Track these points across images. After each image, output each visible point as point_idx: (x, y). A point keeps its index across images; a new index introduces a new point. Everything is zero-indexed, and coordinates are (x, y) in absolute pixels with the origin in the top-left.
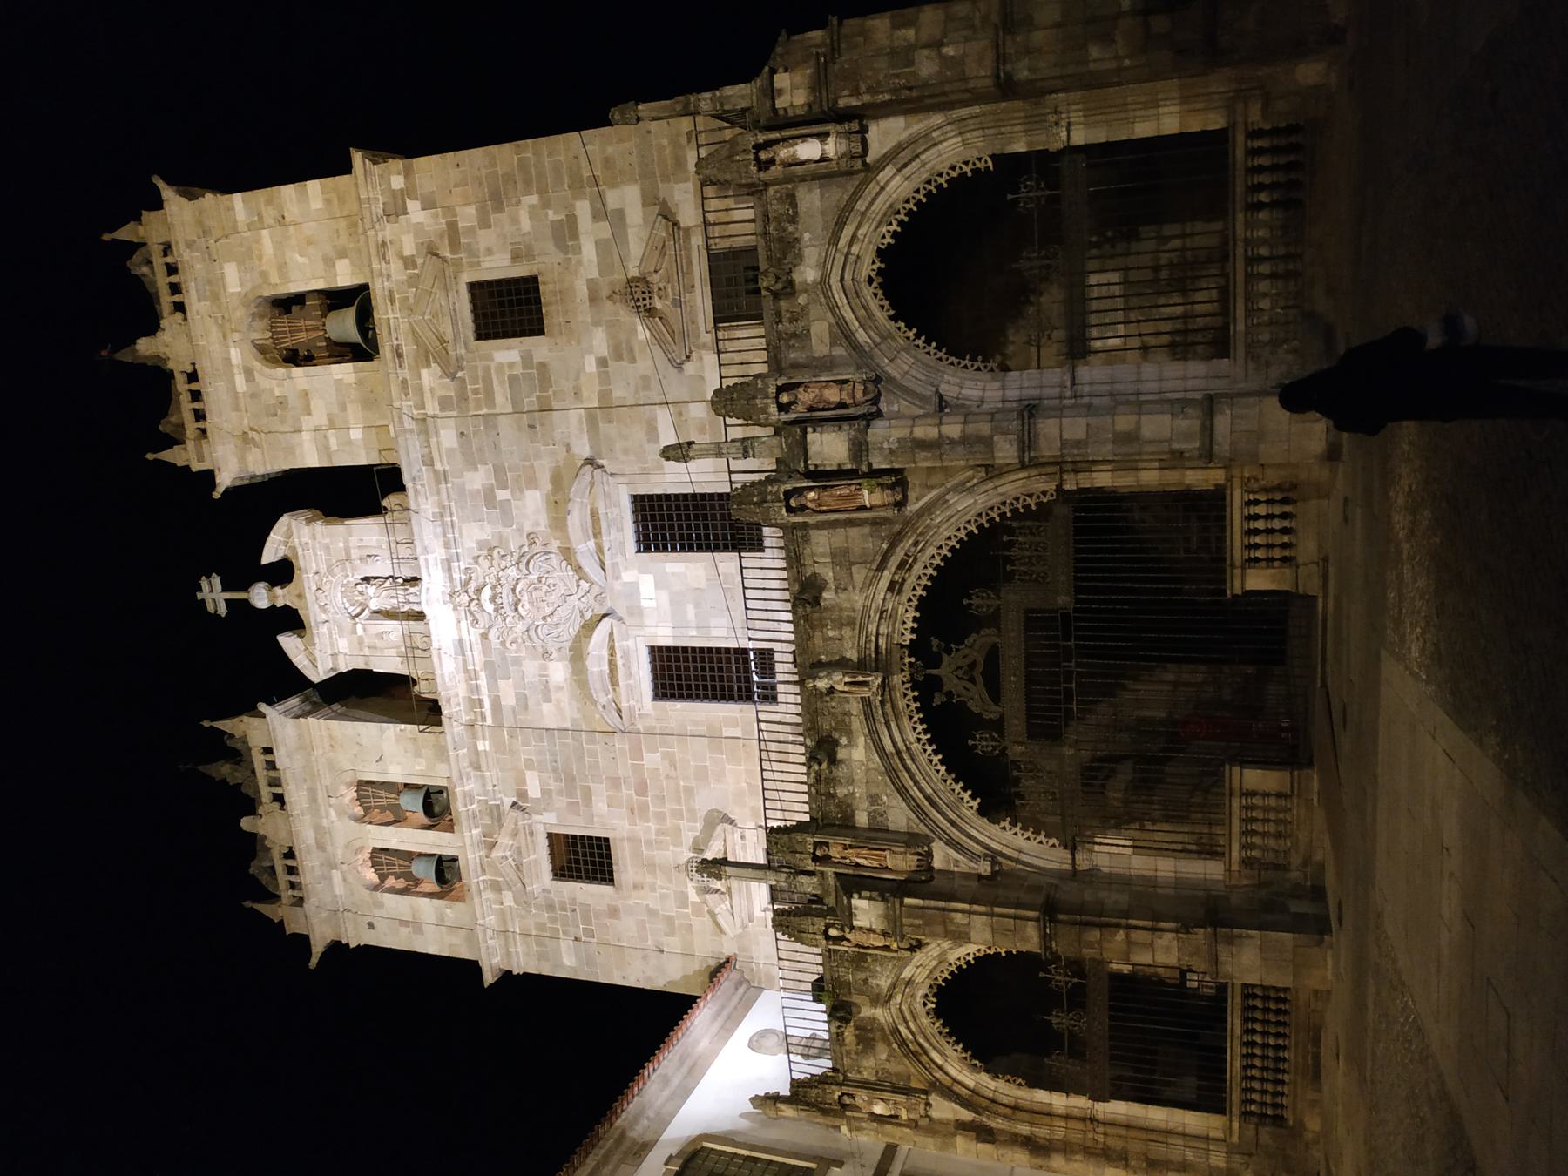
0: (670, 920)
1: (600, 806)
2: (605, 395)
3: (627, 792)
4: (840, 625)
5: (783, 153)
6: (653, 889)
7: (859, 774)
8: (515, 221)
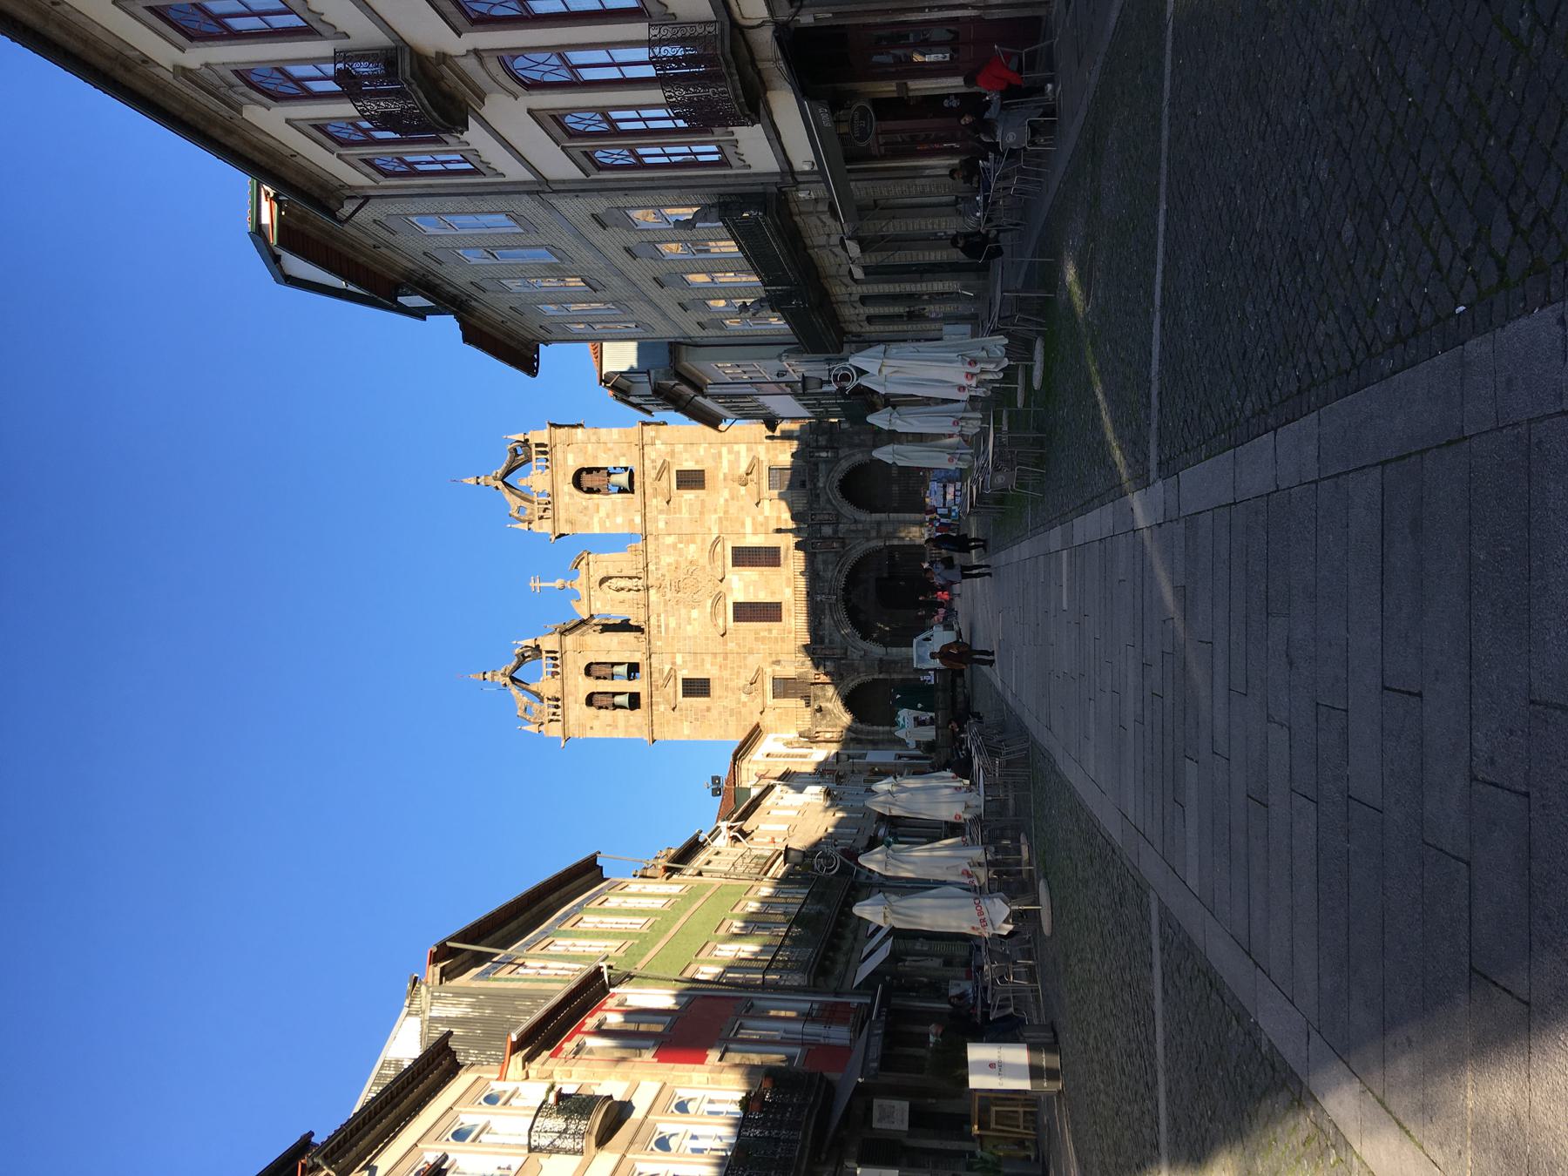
0: (732, 710)
1: (708, 666)
2: (726, 512)
3: (720, 659)
4: (823, 582)
5: (817, 454)
6: (726, 698)
7: (827, 627)
8: (698, 451)
